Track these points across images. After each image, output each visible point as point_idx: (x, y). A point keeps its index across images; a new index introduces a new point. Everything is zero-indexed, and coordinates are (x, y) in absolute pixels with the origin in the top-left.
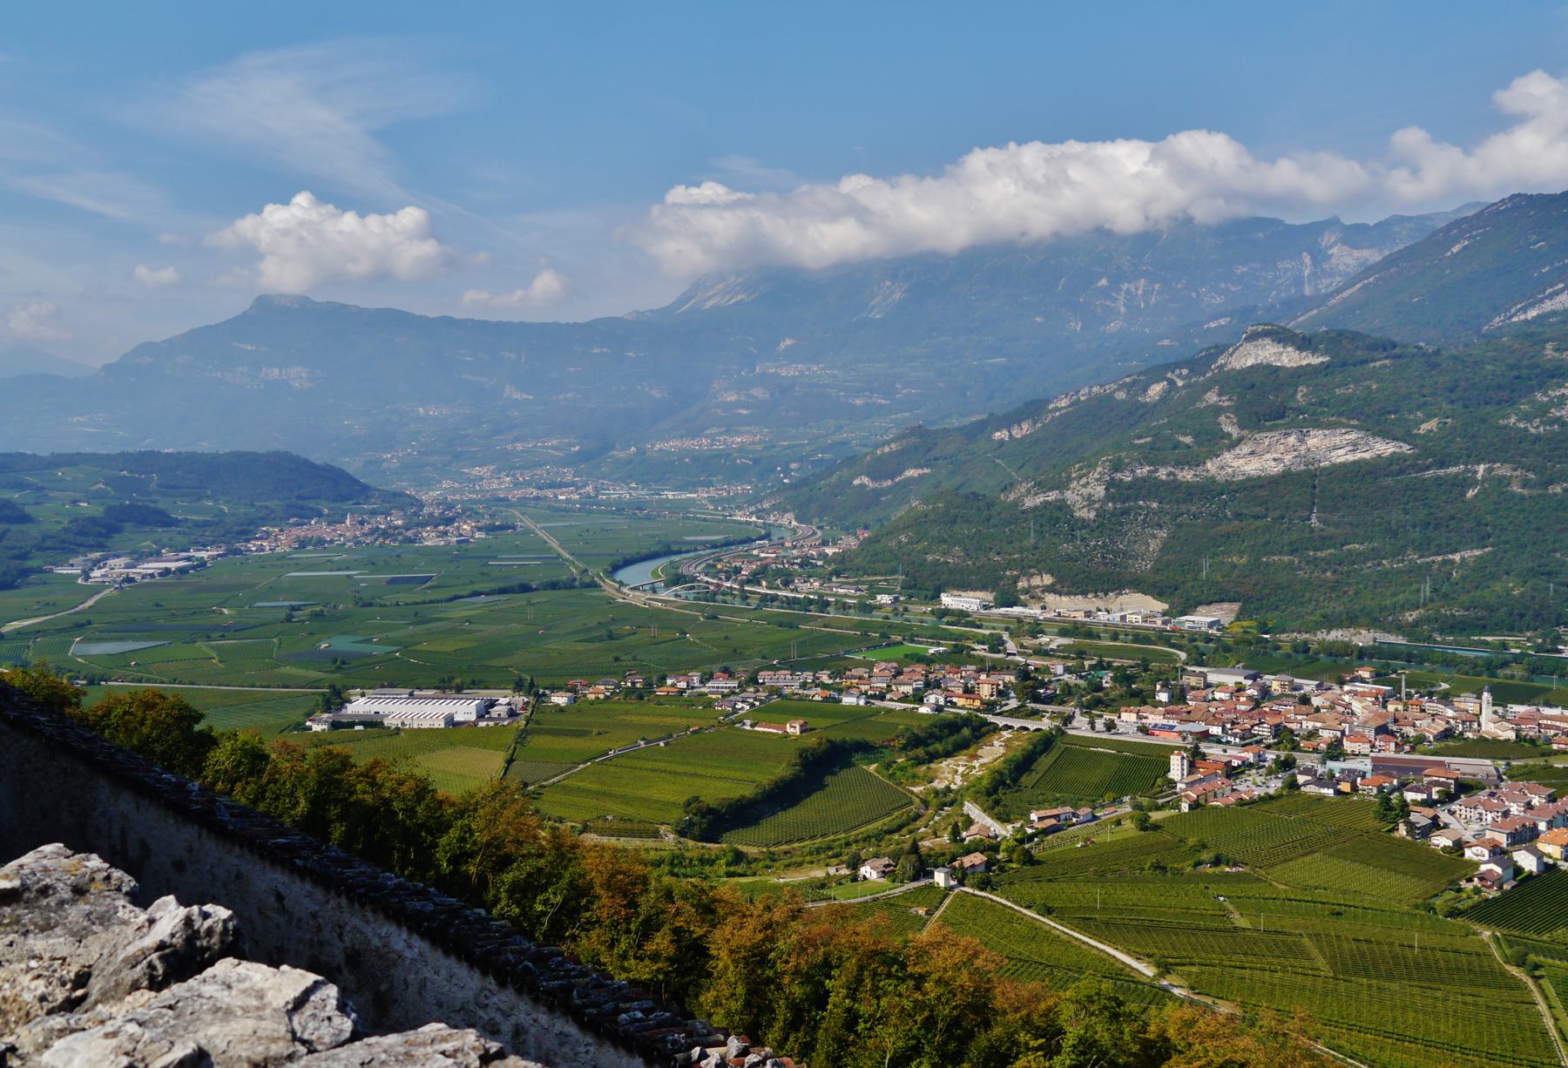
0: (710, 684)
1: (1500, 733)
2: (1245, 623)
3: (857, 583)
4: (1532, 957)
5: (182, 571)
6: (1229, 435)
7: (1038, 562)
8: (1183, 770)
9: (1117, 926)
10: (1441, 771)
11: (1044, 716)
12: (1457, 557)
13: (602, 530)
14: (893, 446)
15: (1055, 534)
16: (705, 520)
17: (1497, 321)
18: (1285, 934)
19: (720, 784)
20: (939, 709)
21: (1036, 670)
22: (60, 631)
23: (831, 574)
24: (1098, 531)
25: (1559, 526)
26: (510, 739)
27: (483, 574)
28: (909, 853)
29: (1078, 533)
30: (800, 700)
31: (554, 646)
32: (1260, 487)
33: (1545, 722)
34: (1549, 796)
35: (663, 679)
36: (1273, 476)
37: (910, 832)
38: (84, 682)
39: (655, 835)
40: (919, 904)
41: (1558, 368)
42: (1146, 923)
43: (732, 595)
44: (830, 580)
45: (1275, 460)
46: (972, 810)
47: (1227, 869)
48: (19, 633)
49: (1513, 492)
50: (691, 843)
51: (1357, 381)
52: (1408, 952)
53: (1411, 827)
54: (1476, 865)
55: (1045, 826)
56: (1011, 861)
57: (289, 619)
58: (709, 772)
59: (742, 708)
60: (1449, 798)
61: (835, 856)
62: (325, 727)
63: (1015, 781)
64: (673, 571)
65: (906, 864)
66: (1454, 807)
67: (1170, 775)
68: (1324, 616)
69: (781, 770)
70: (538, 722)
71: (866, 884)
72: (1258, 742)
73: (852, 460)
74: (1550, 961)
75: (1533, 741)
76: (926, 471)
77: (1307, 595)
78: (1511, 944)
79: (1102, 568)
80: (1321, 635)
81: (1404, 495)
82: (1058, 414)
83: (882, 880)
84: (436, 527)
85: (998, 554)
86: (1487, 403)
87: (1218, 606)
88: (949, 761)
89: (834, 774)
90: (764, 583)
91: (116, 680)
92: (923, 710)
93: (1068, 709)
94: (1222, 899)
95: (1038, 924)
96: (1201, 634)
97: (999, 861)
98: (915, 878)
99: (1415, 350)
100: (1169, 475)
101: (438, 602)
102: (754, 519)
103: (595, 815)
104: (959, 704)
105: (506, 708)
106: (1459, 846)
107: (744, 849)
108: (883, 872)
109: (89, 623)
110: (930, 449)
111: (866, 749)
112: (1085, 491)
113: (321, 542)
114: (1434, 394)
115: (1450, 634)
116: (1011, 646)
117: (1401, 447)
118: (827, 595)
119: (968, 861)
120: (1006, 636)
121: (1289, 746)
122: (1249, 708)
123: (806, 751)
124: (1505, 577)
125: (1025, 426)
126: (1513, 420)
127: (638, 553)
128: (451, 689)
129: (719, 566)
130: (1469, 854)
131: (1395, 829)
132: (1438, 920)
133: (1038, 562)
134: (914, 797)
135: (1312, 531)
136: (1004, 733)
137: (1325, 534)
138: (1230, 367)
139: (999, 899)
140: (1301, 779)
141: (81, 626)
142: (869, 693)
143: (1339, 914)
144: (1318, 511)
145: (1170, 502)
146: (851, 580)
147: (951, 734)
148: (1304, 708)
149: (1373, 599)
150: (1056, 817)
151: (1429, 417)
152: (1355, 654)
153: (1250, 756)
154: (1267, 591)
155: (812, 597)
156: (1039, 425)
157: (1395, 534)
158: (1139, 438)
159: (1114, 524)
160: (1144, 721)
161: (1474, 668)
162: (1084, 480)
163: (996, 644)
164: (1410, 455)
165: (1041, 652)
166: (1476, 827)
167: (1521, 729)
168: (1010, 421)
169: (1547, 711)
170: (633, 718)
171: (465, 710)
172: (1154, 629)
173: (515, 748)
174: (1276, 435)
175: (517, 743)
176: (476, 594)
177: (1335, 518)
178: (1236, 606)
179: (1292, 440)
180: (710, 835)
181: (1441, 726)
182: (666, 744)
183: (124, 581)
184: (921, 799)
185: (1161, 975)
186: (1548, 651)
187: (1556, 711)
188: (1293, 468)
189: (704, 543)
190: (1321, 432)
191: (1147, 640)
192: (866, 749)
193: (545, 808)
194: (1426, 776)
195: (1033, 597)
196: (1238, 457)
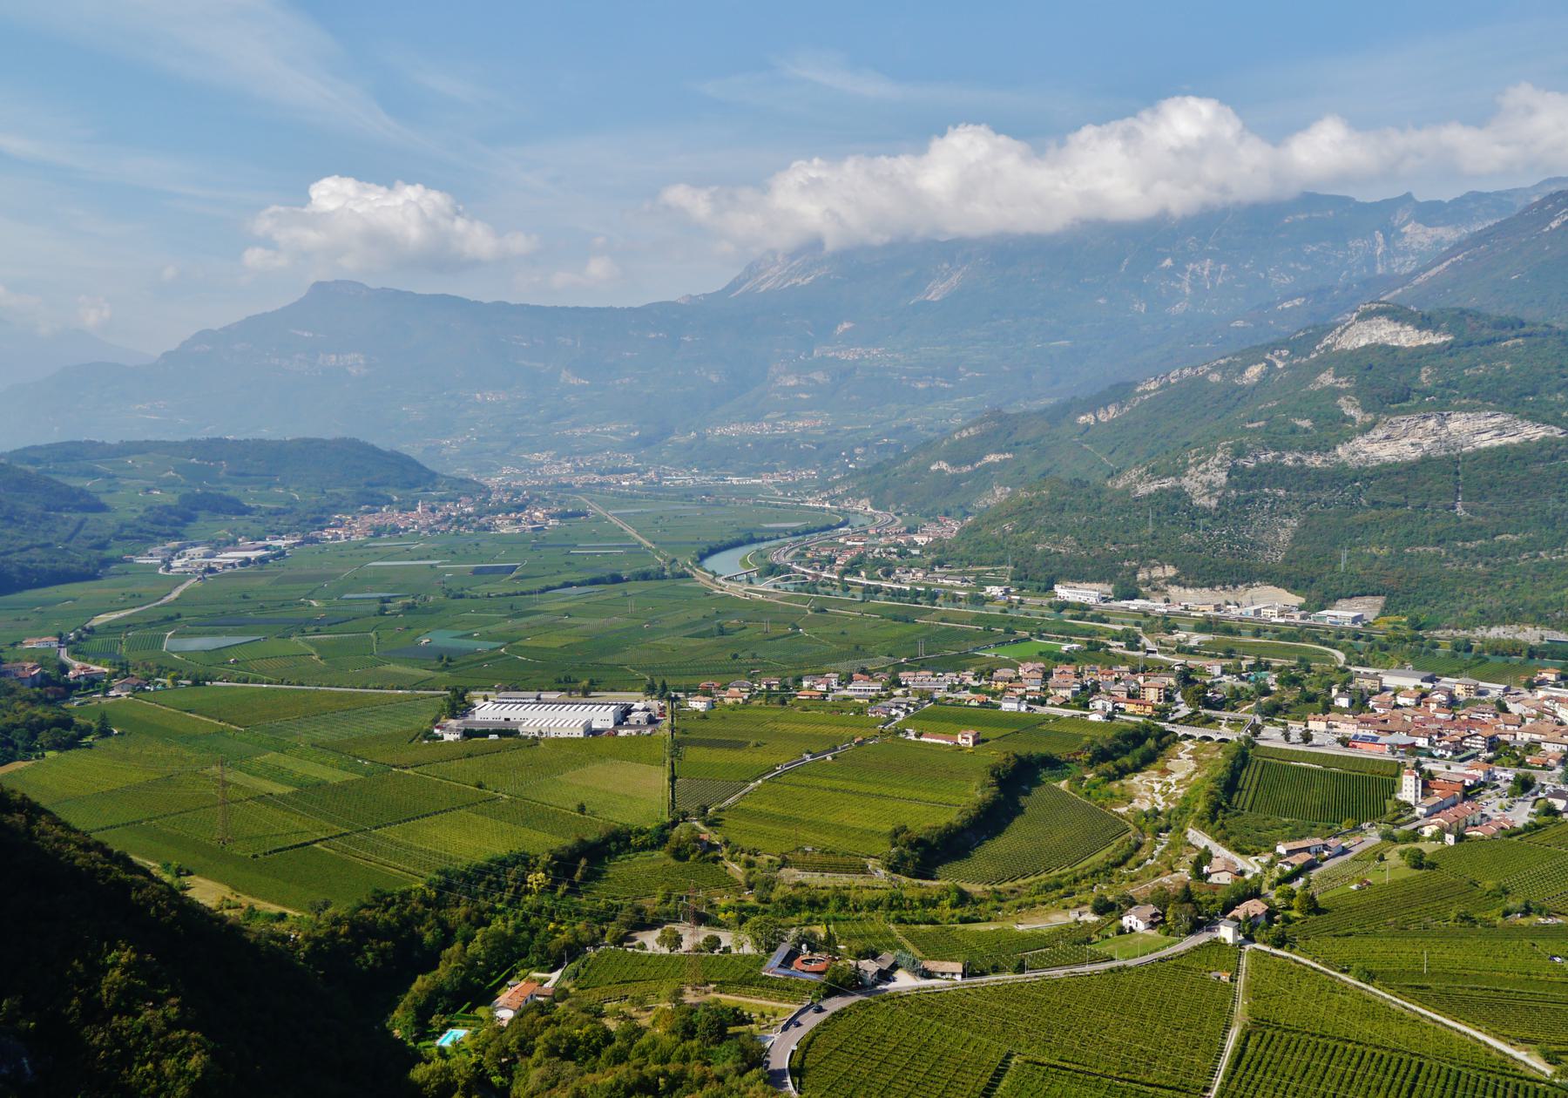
0: (851, 687)
2: (1393, 619)
3: (962, 574)
5: (262, 560)
6: (1352, 419)
7: (1159, 552)
8: (1417, 791)
11: (1220, 724)
14: (971, 430)
15: (1174, 523)
16: (777, 506)
19: (914, 807)
22: (150, 624)
23: (933, 564)
24: (1221, 521)
27: (568, 563)
31: (664, 642)
32: (1397, 474)
35: (799, 680)
36: (1411, 462)
37: (1139, 865)
38: (189, 682)
39: (863, 870)
44: (933, 570)
45: (1412, 445)
48: (110, 628)
50: (905, 880)
51: (1488, 361)
56: (1290, 908)
57: (382, 612)
59: (897, 715)
61: (1070, 894)
62: (458, 736)
63: (1229, 802)
64: (763, 561)
68: (1483, 612)
69: (975, 793)
70: (684, 732)
73: (928, 445)
76: (1008, 456)
77: (1459, 589)
79: (1229, 559)
80: (1480, 632)
81: (1558, 483)
82: (1147, 397)
83: (1151, 932)
84: (507, 514)
87: (1360, 600)
89: (1027, 794)
90: (863, 574)
91: (220, 681)
92: (1094, 717)
94: (1558, 960)
96: (1348, 630)
99: (1545, 329)
100: (1295, 460)
101: (531, 593)
102: (827, 505)
103: (793, 847)
104: (1128, 710)
105: (646, 715)
107: (967, 887)
108: (1151, 922)
109: (179, 616)
110: (1010, 434)
111: (1052, 764)
112: (1205, 478)
113: (395, 530)
116: (1145, 640)
117: (1552, 431)
118: (934, 586)
121: (1513, 762)
125: (1112, 410)
127: (722, 541)
128: (577, 691)
129: (809, 555)
133: (1159, 552)
135: (1459, 520)
136: (1185, 743)
137: (1474, 523)
138: (1338, 347)
142: (1028, 697)
144: (1463, 500)
145: (1298, 489)
146: (956, 571)
147: (1137, 746)
149: (1533, 594)
150: (1307, 850)
152: (1525, 653)
153: (1480, 774)
154: (1413, 584)
156: (1127, 409)
157: (1551, 523)
162: (1202, 467)
163: (1133, 642)
164: (1563, 440)
165: (1182, 650)
168: (1093, 405)
170: (785, 726)
172: (1295, 625)
173: (673, 764)
174: (1414, 418)
176: (568, 585)
177: (1483, 507)
178: (1380, 601)
179: (1431, 423)
180: (924, 871)
182: (834, 758)
183: (206, 571)
188: (1432, 454)
189: (785, 530)
190: (1463, 415)
191: (1292, 637)
192: (1052, 764)
193: (736, 838)
195: (1155, 590)
196: (1371, 441)
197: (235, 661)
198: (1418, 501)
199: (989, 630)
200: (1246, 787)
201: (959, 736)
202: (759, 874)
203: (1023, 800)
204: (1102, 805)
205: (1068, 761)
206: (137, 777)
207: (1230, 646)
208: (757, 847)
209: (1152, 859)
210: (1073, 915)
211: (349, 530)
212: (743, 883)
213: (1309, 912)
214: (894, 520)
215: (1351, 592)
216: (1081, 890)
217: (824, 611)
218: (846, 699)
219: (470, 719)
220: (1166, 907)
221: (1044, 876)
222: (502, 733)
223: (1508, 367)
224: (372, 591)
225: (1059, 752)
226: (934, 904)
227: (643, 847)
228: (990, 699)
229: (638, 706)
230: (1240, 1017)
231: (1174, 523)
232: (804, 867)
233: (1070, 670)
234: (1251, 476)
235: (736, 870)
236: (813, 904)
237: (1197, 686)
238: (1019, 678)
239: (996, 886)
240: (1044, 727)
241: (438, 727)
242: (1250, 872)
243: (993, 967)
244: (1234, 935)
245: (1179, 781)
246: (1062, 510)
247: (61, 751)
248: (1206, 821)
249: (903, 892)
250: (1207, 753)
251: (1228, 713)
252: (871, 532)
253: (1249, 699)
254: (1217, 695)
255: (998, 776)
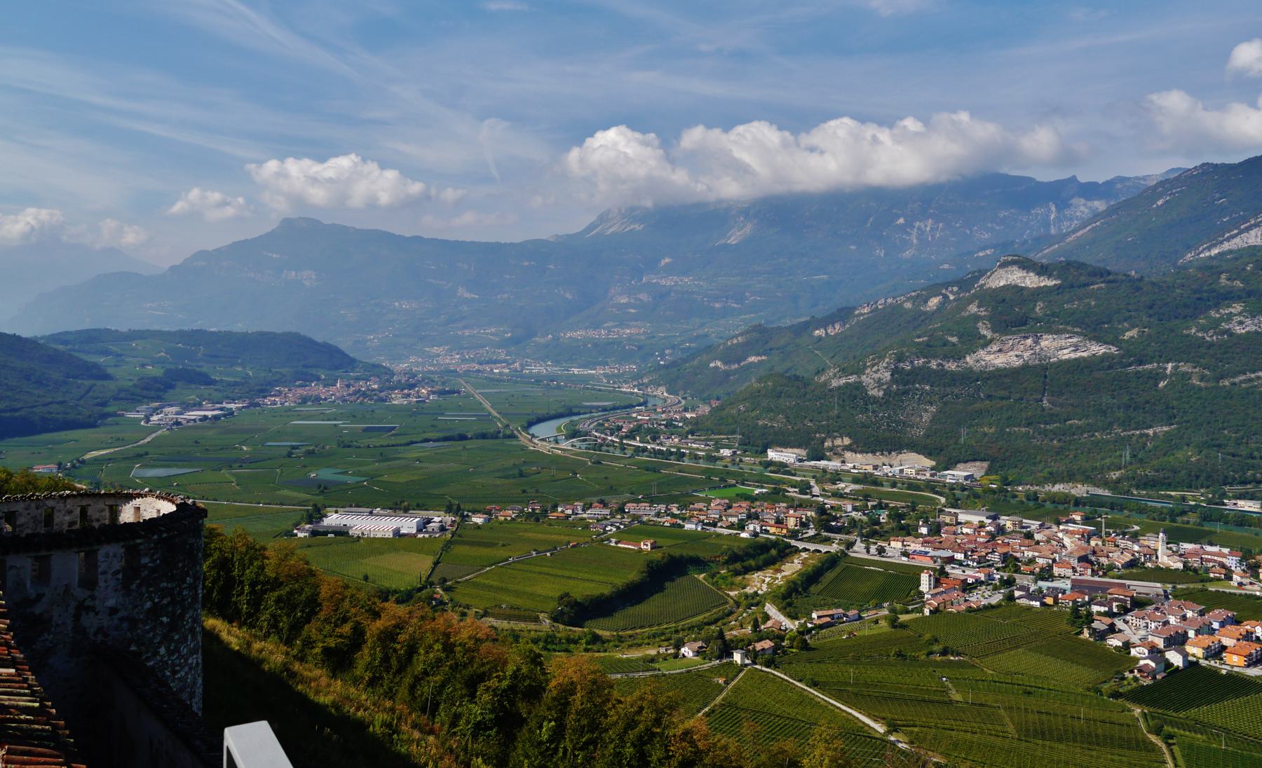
0: (589, 512)
1: (1172, 564)
4: (1168, 729)
5: (216, 418)
6: (985, 336)
8: (930, 584)
9: (863, 696)
10: (1121, 591)
12: (1151, 432)
13: (524, 396)
14: (740, 339)
15: (853, 407)
16: (600, 390)
17: (1189, 256)
18: (987, 706)
19: (587, 584)
20: (755, 534)
21: (832, 507)
23: (688, 433)
25: (1227, 410)
26: (438, 547)
27: (433, 426)
28: (717, 638)
29: (870, 407)
30: (654, 525)
31: (480, 480)
32: (1005, 376)
33: (1206, 556)
34: (1201, 611)
35: (555, 507)
39: (536, 620)
40: (721, 676)
41: (1230, 292)
42: (885, 695)
44: (687, 437)
45: (1017, 356)
46: (771, 609)
47: (952, 658)
48: (96, 460)
49: (1194, 384)
50: (561, 627)
51: (1080, 299)
52: (1076, 723)
53: (1094, 632)
54: (1137, 660)
55: (821, 623)
56: (792, 647)
57: (289, 455)
58: (581, 575)
60: (1125, 610)
61: (667, 640)
62: (307, 534)
63: (805, 589)
64: (572, 428)
65: (715, 646)
66: (1128, 618)
67: (921, 588)
68: (1051, 473)
69: (633, 576)
70: (460, 536)
71: (684, 661)
72: (989, 566)
73: (709, 349)
74: (1182, 732)
75: (1195, 570)
76: (763, 358)
77: (1038, 458)
78: (1153, 718)
79: (887, 434)
80: (1048, 488)
81: (1112, 385)
82: (862, 318)
84: (402, 390)
85: (811, 421)
86: (1176, 318)
87: (973, 464)
88: (760, 573)
89: (673, 580)
90: (638, 438)
92: (744, 535)
93: (852, 537)
94: (944, 679)
95: (806, 693)
97: (784, 647)
98: (720, 657)
99: (1124, 278)
100: (939, 365)
101: (397, 445)
102: (636, 390)
103: (493, 604)
104: (771, 532)
106: (1127, 645)
109: (147, 454)
110: (766, 343)
111: (699, 564)
112: (876, 376)
113: (317, 400)
114: (1136, 310)
115: (1144, 489)
116: (816, 490)
117: (1110, 349)
119: (759, 646)
120: (812, 483)
122: (985, 540)
123: (651, 562)
124: (1185, 447)
125: (837, 326)
126: (1193, 331)
128: (400, 509)
129: (606, 425)
130: (1133, 652)
131: (1081, 633)
132: (1103, 700)
134: (729, 599)
135: (1043, 409)
138: (988, 286)
139: (779, 674)
140: (1017, 594)
143: (1029, 693)
145: (939, 385)
147: (762, 553)
148: (1027, 542)
149: (1087, 461)
150: (832, 616)
151: (1133, 327)
152: (1072, 502)
153: (982, 576)
154: (1007, 454)
155: (672, 450)
156: (847, 326)
157: (1104, 413)
158: (919, 337)
160: (907, 548)
161: (1161, 515)
162: (875, 368)
163: (805, 488)
164: (1116, 355)
166: (1142, 633)
167: (1188, 562)
168: (825, 322)
169: (1209, 548)
171: (408, 525)
175: (443, 550)
176: (427, 440)
177: (1061, 400)
178: (985, 464)
179: (1029, 341)
181: (1128, 557)
182: (551, 555)
183: (174, 424)
184: (734, 600)
185: (889, 732)
186: (1217, 504)
187: (1215, 549)
191: (918, 488)
192: (699, 564)
193: (458, 598)
194: (1109, 594)
195: (835, 454)
196: (989, 353)
197: (178, 485)
198: (1018, 396)
205: (709, 561)
208: (470, 604)
211: (283, 399)
213: (802, 649)
214: (680, 402)
215: (966, 458)
217: (600, 463)
219: (322, 524)
223: (1093, 304)
224: (287, 441)
225: (703, 555)
226: (575, 642)
231: (853, 407)
234: (908, 375)
246: (779, 397)
252: (659, 410)
255: (652, 568)
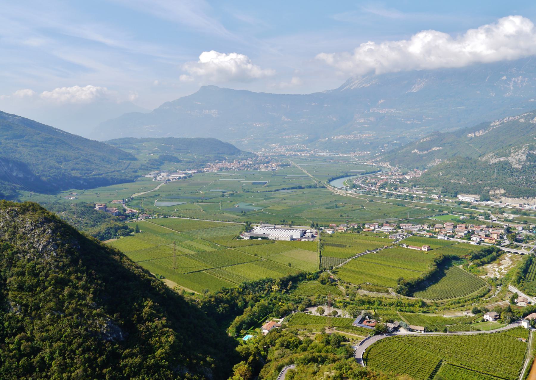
0: (383, 228)
3: (423, 190)
5: (185, 178)
7: (498, 184)
11: (521, 248)
13: (320, 167)
15: (504, 174)
16: (356, 164)
19: (406, 271)
22: (150, 197)
23: (413, 186)
31: (316, 209)
35: (364, 225)
37: (489, 297)
38: (163, 216)
39: (387, 292)
43: (376, 192)
48: (138, 198)
50: (402, 297)
57: (223, 196)
58: (399, 266)
59: (399, 239)
61: (463, 306)
62: (248, 238)
63: (525, 277)
69: (428, 268)
70: (324, 241)
73: (411, 143)
76: (441, 148)
79: (526, 188)
82: (495, 127)
84: (263, 164)
85: (481, 181)
89: (447, 269)
90: (387, 188)
91: (172, 216)
92: (473, 243)
102: (374, 164)
103: (362, 282)
104: (485, 241)
107: (425, 301)
108: (495, 318)
109: (159, 195)
110: (442, 140)
111: (456, 258)
112: (517, 158)
113: (227, 169)
116: (492, 216)
125: (481, 132)
127: (336, 176)
128: (288, 225)
129: (367, 181)
133: (498, 184)
136: (508, 254)
141: (157, 196)
142: (447, 235)
146: (421, 189)
147: (489, 254)
159: (530, 171)
162: (517, 153)
163: (487, 217)
165: (506, 220)
168: (474, 130)
170: (359, 240)
173: (320, 252)
176: (284, 189)
180: (409, 294)
182: (377, 252)
183: (167, 181)
189: (359, 173)
193: (342, 278)
195: (496, 198)
197: (177, 210)
199: (433, 210)
200: (532, 271)
201: (422, 247)
202: (350, 291)
203: (446, 271)
204: (476, 275)
205: (462, 258)
206: (147, 246)
207: (526, 220)
209: (495, 295)
210: (464, 313)
211: (212, 169)
212: (345, 293)
216: (468, 305)
218: (381, 232)
219: (252, 232)
220: (501, 313)
221: (453, 299)
222: (262, 238)
226: (413, 306)
227: (311, 279)
228: (433, 235)
229: (308, 231)
230: (530, 355)
231: (504, 174)
232: (366, 290)
233: (464, 225)
235: (343, 289)
236: (369, 302)
237: (512, 234)
238: (444, 228)
239: (436, 301)
240: (454, 246)
241: (241, 235)
242: (533, 303)
243: (435, 329)
244: (528, 325)
245: (505, 268)
247: (125, 236)
248: (516, 283)
249: (402, 301)
250: (516, 258)
251: (525, 244)
252: (390, 174)
253: (533, 239)
254: (520, 237)
255: (437, 262)
